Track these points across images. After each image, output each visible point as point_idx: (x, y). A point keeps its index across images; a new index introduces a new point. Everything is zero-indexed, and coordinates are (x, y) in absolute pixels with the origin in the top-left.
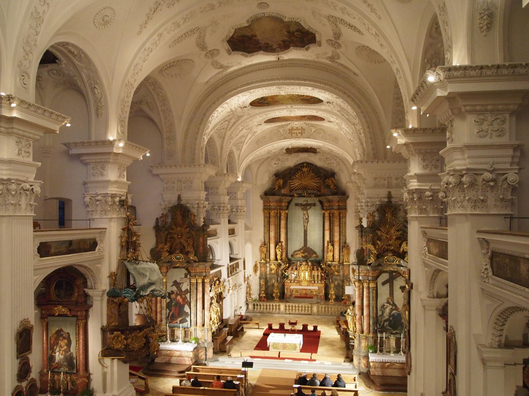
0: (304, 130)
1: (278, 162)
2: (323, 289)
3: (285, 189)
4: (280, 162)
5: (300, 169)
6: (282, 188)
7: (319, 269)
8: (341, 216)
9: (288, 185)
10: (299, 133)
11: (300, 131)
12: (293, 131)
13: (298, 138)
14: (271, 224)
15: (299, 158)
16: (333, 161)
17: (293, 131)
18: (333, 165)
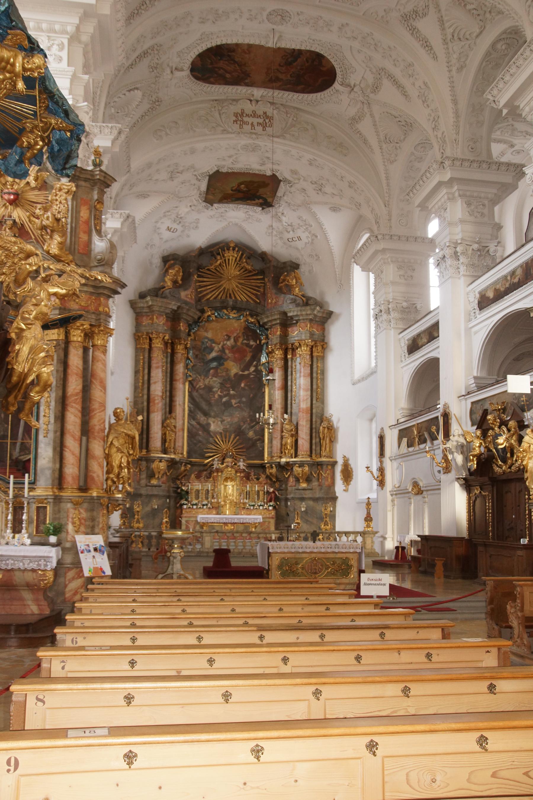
0: (271, 118)
1: (175, 226)
2: (273, 522)
3: (188, 292)
4: (179, 227)
5: (219, 254)
6: (180, 286)
7: (263, 478)
8: (315, 354)
9: (193, 285)
10: (259, 124)
11: (261, 121)
12: (246, 119)
13: (255, 134)
14: (154, 365)
15: (224, 224)
16: (300, 233)
17: (246, 119)
18: (299, 245)
